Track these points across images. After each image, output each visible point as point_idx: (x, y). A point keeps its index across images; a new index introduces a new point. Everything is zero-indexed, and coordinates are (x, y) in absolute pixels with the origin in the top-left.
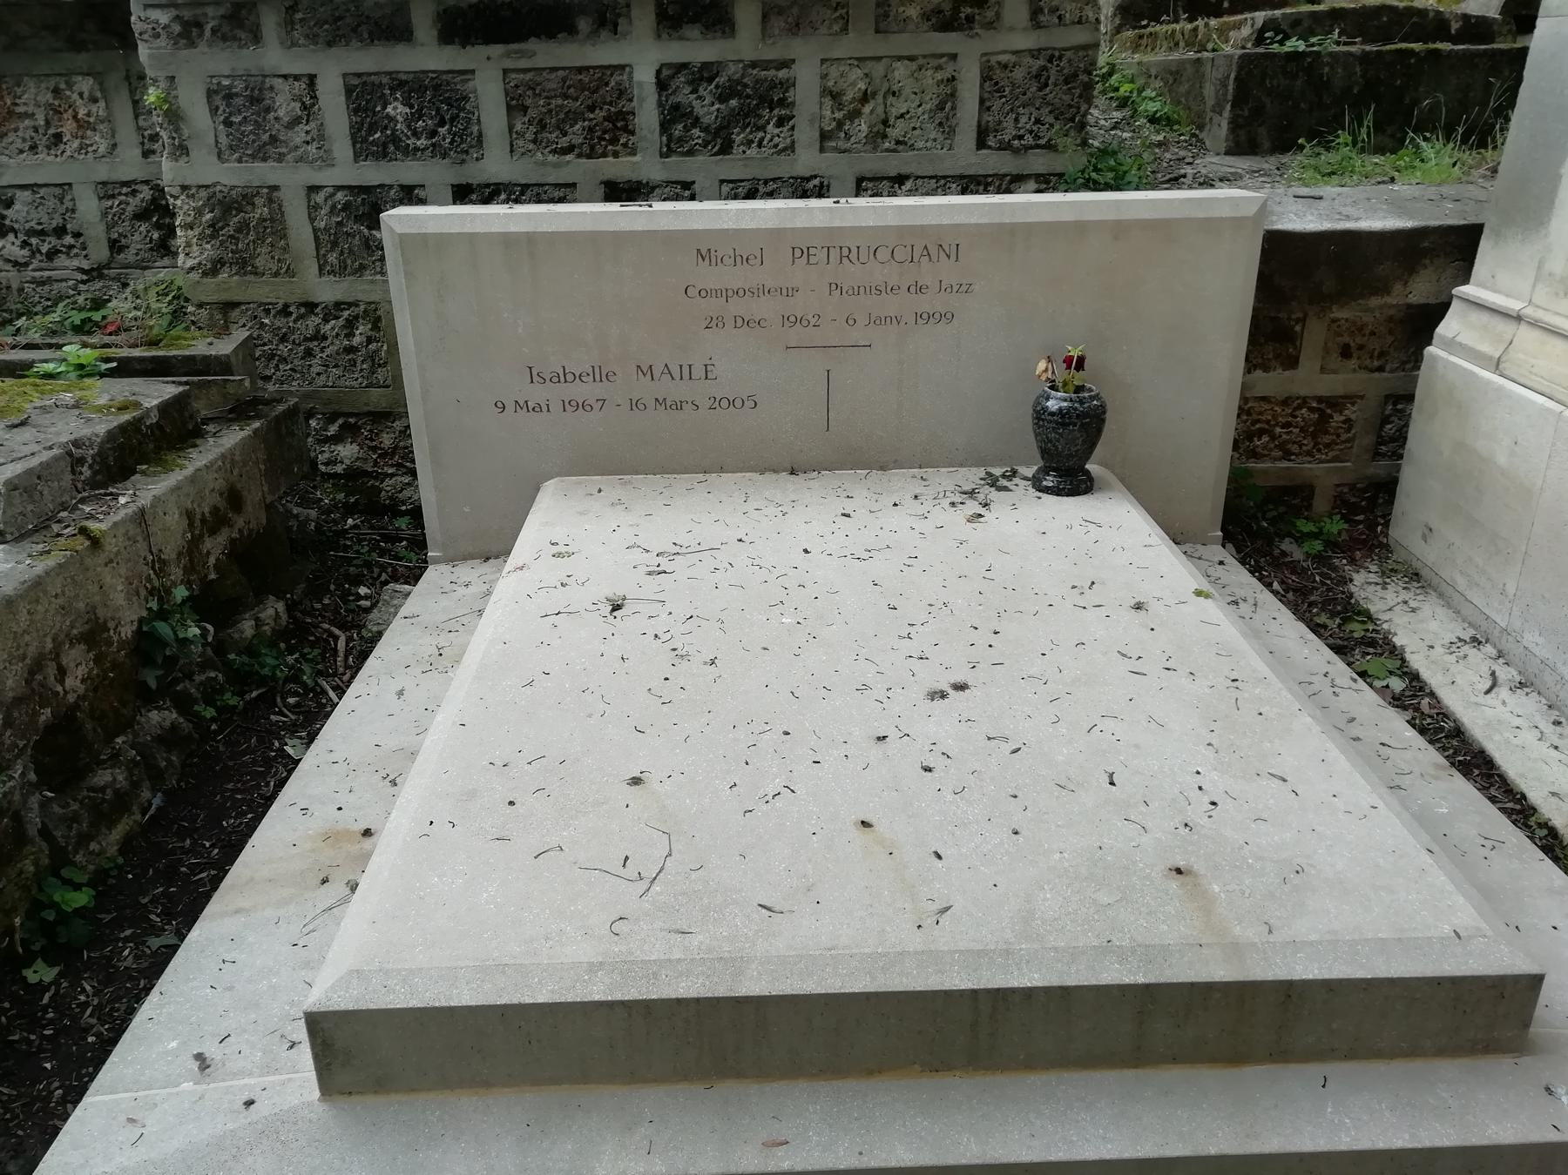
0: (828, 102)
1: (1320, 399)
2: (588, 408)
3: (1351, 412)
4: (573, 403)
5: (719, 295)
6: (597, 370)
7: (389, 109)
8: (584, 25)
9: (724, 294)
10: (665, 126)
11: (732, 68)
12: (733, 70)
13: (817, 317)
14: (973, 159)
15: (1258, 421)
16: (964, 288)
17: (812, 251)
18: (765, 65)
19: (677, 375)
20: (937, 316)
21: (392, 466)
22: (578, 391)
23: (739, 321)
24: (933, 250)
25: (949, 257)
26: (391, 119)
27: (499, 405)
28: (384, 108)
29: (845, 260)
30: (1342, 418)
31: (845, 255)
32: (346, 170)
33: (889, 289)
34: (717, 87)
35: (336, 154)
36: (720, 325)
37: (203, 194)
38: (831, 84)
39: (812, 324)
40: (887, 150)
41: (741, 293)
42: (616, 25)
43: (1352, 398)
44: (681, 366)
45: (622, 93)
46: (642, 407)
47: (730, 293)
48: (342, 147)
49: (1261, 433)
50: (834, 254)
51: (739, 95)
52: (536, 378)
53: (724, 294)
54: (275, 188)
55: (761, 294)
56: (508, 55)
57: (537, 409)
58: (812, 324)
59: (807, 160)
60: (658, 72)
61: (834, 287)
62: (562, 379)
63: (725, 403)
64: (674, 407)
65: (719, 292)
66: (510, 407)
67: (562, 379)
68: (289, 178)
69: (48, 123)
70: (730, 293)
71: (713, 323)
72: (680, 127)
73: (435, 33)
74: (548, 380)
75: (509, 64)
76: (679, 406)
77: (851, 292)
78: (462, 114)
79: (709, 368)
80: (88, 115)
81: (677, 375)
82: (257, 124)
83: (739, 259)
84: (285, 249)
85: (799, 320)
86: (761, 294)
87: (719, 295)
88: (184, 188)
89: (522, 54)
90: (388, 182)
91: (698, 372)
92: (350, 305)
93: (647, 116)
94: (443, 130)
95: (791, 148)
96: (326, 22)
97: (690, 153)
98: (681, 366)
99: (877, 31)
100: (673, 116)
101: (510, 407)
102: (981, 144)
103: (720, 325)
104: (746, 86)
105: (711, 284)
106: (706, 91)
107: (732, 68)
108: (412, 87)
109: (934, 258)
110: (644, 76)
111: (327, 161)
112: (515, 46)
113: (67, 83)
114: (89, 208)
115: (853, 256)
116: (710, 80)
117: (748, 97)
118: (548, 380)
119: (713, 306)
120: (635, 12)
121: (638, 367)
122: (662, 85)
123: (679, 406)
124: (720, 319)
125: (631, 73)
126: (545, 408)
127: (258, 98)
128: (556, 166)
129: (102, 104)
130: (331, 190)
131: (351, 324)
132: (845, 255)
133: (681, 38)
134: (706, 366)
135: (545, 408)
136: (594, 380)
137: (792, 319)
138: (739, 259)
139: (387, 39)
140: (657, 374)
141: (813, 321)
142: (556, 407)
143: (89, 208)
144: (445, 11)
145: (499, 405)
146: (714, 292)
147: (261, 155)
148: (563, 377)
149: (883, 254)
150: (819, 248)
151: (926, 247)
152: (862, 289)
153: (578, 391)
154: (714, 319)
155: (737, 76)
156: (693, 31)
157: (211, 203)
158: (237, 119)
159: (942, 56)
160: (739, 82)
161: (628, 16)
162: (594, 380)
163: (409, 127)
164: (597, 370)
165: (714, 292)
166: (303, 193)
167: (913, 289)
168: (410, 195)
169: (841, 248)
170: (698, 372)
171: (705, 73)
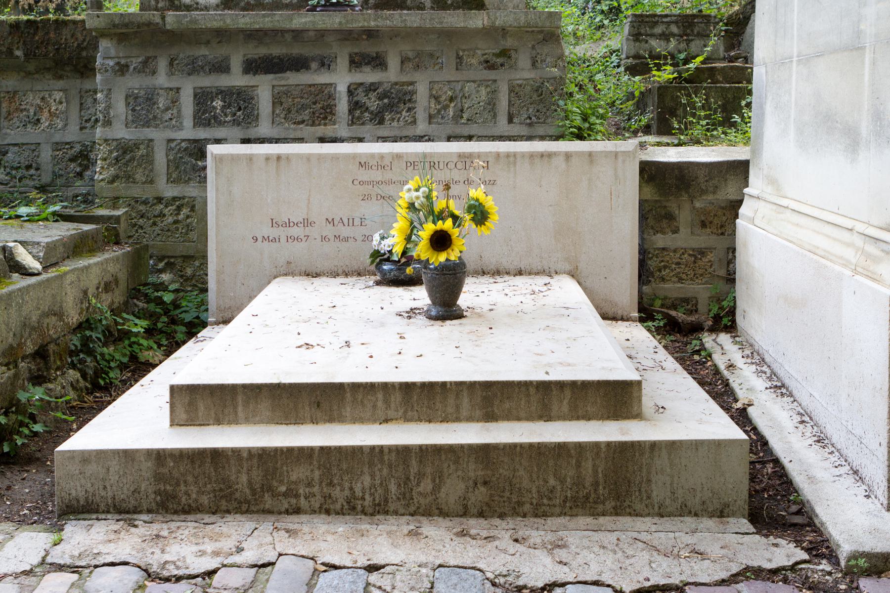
0: (433, 101)
1: (693, 250)
2: (300, 240)
3: (710, 257)
4: (292, 238)
6: (306, 221)
7: (214, 103)
8: (314, 65)
10: (350, 112)
11: (386, 85)
12: (387, 86)
15: (662, 261)
16: (492, 182)
17: (416, 163)
18: (403, 84)
19: (346, 224)
21: (190, 286)
22: (295, 231)
23: (379, 197)
26: (215, 108)
28: (212, 103)
29: (432, 168)
30: (707, 260)
32: (188, 131)
34: (378, 94)
35: (185, 124)
36: (369, 198)
37: (115, 143)
38: (434, 92)
40: (463, 124)
41: (380, 183)
42: (329, 66)
43: (711, 249)
45: (331, 96)
46: (327, 240)
47: (375, 183)
48: (188, 122)
49: (665, 267)
50: (427, 165)
51: (389, 97)
54: (151, 140)
56: (276, 79)
59: (422, 127)
60: (349, 87)
66: (260, 239)
68: (158, 135)
69: (35, 114)
70: (375, 183)
71: (366, 198)
72: (358, 112)
73: (241, 69)
75: (275, 83)
76: (346, 239)
78: (250, 106)
80: (57, 110)
81: (346, 224)
82: (148, 111)
83: (379, 167)
84: (151, 170)
88: (106, 140)
89: (283, 78)
90: (208, 137)
91: (357, 222)
92: (180, 198)
93: (342, 106)
94: (239, 113)
95: (414, 122)
96: (189, 65)
97: (363, 124)
99: (457, 69)
100: (355, 106)
101: (260, 239)
102: (510, 121)
103: (369, 198)
104: (392, 93)
105: (365, 178)
106: (373, 95)
107: (386, 85)
108: (226, 94)
110: (342, 88)
111: (180, 128)
112: (277, 75)
113: (49, 94)
114: (46, 155)
116: (375, 90)
117: (393, 98)
120: (339, 60)
122: (350, 92)
123: (346, 239)
125: (335, 87)
126: (277, 240)
127: (150, 99)
128: (295, 130)
129: (64, 104)
130: (179, 141)
131: (179, 208)
133: (361, 72)
135: (277, 240)
138: (379, 167)
139: (218, 72)
140: (336, 223)
142: (283, 239)
143: (46, 155)
144: (247, 60)
147: (147, 124)
148: (288, 224)
153: (295, 231)
155: (388, 89)
156: (367, 69)
157: (117, 149)
158: (138, 108)
159: (489, 80)
160: (389, 92)
161: (336, 62)
163: (222, 112)
164: (306, 221)
166: (165, 143)
167: (466, 182)
168: (218, 141)
170: (357, 222)
171: (372, 88)
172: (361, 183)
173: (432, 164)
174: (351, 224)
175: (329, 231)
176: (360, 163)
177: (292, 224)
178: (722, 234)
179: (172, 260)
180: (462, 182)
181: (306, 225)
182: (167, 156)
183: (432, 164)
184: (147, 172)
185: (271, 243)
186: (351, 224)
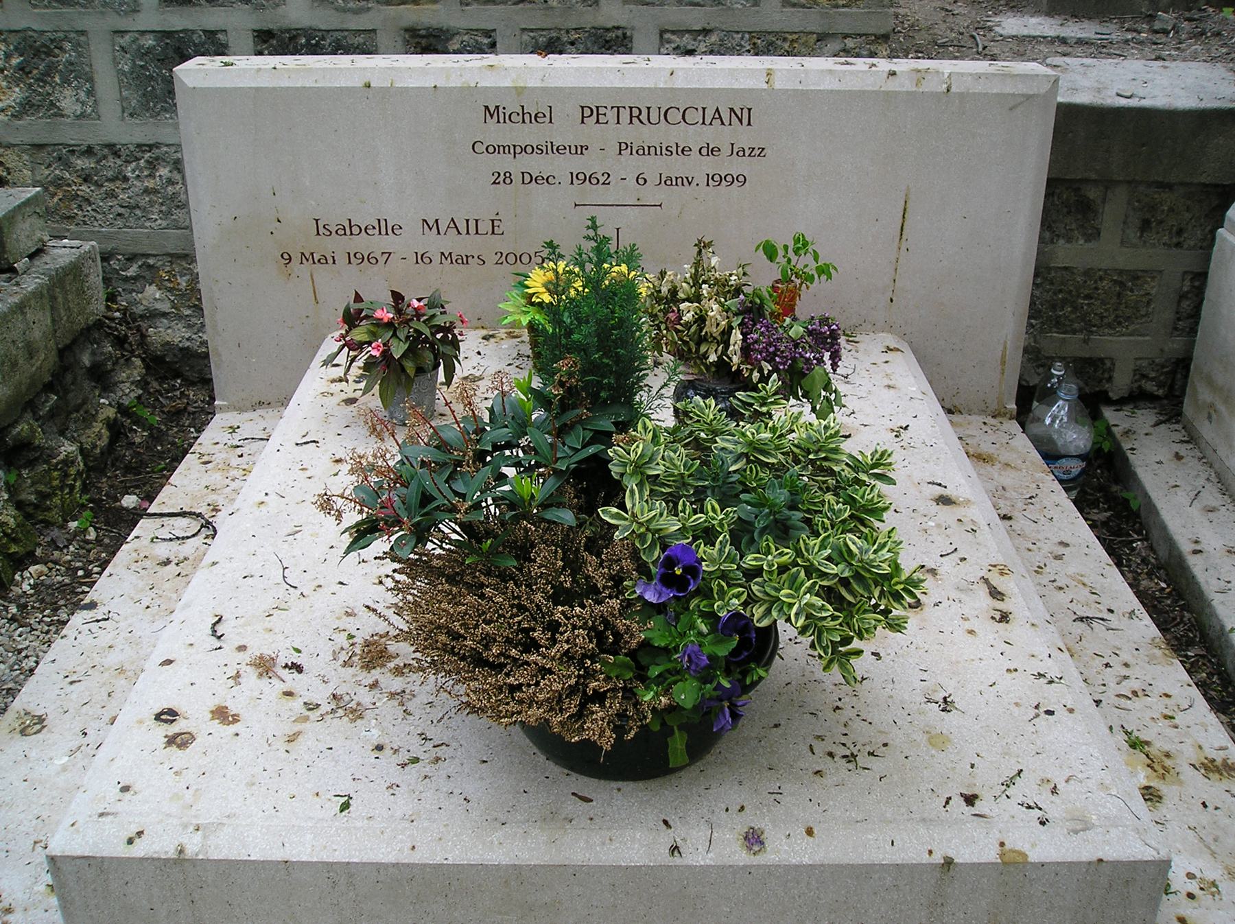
1: (1121, 272)
2: (373, 261)
3: (1153, 287)
5: (507, 151)
6: (383, 223)
9: (512, 151)
13: (606, 176)
14: (777, 17)
15: (1061, 291)
16: (757, 152)
17: (602, 111)
19: (463, 231)
20: (729, 178)
22: (361, 243)
24: (725, 116)
25: (741, 121)
27: (286, 256)
29: (635, 120)
30: (1142, 293)
31: (635, 115)
33: (680, 149)
36: (508, 181)
37: (14, 39)
39: (601, 182)
41: (529, 150)
43: (1154, 273)
44: (467, 221)
47: (518, 150)
49: (1064, 302)
50: (625, 115)
52: (322, 230)
53: (512, 151)
55: (550, 151)
57: (323, 260)
58: (601, 182)
61: (623, 146)
62: (348, 232)
63: (511, 259)
64: (460, 261)
65: (507, 148)
66: (296, 258)
67: (348, 232)
70: (518, 150)
74: (334, 233)
76: (465, 260)
77: (641, 152)
79: (496, 223)
81: (463, 231)
83: (527, 117)
84: (90, 93)
85: (589, 179)
86: (550, 151)
87: (507, 151)
90: (190, 27)
91: (485, 227)
92: (151, 147)
98: (467, 221)
101: (296, 258)
103: (508, 181)
109: (726, 122)
115: (644, 117)
118: (334, 233)
119: (504, 163)
121: (424, 221)
123: (465, 260)
124: (508, 175)
126: (330, 261)
131: (152, 165)
132: (635, 115)
134: (493, 221)
135: (330, 261)
136: (380, 233)
137: (581, 177)
138: (527, 117)
140: (442, 229)
141: (602, 180)
142: (342, 260)
145: (286, 256)
146: (501, 148)
148: (348, 229)
149: (675, 116)
150: (609, 108)
151: (717, 110)
152: (652, 149)
154: (502, 174)
162: (380, 233)
164: (383, 223)
165: (501, 148)
167: (704, 151)
169: (631, 108)
170: (485, 227)
172: (491, 149)
173: (635, 112)
174: (472, 229)
175: (434, 244)
176: (487, 107)
177: (356, 230)
178: (1178, 245)
179: (151, 261)
180: (696, 149)
181: (383, 231)
182: (115, 62)
183: (635, 112)
184: (82, 95)
185: (318, 265)
186: (472, 229)
